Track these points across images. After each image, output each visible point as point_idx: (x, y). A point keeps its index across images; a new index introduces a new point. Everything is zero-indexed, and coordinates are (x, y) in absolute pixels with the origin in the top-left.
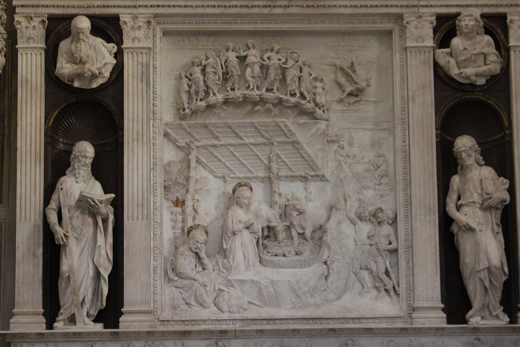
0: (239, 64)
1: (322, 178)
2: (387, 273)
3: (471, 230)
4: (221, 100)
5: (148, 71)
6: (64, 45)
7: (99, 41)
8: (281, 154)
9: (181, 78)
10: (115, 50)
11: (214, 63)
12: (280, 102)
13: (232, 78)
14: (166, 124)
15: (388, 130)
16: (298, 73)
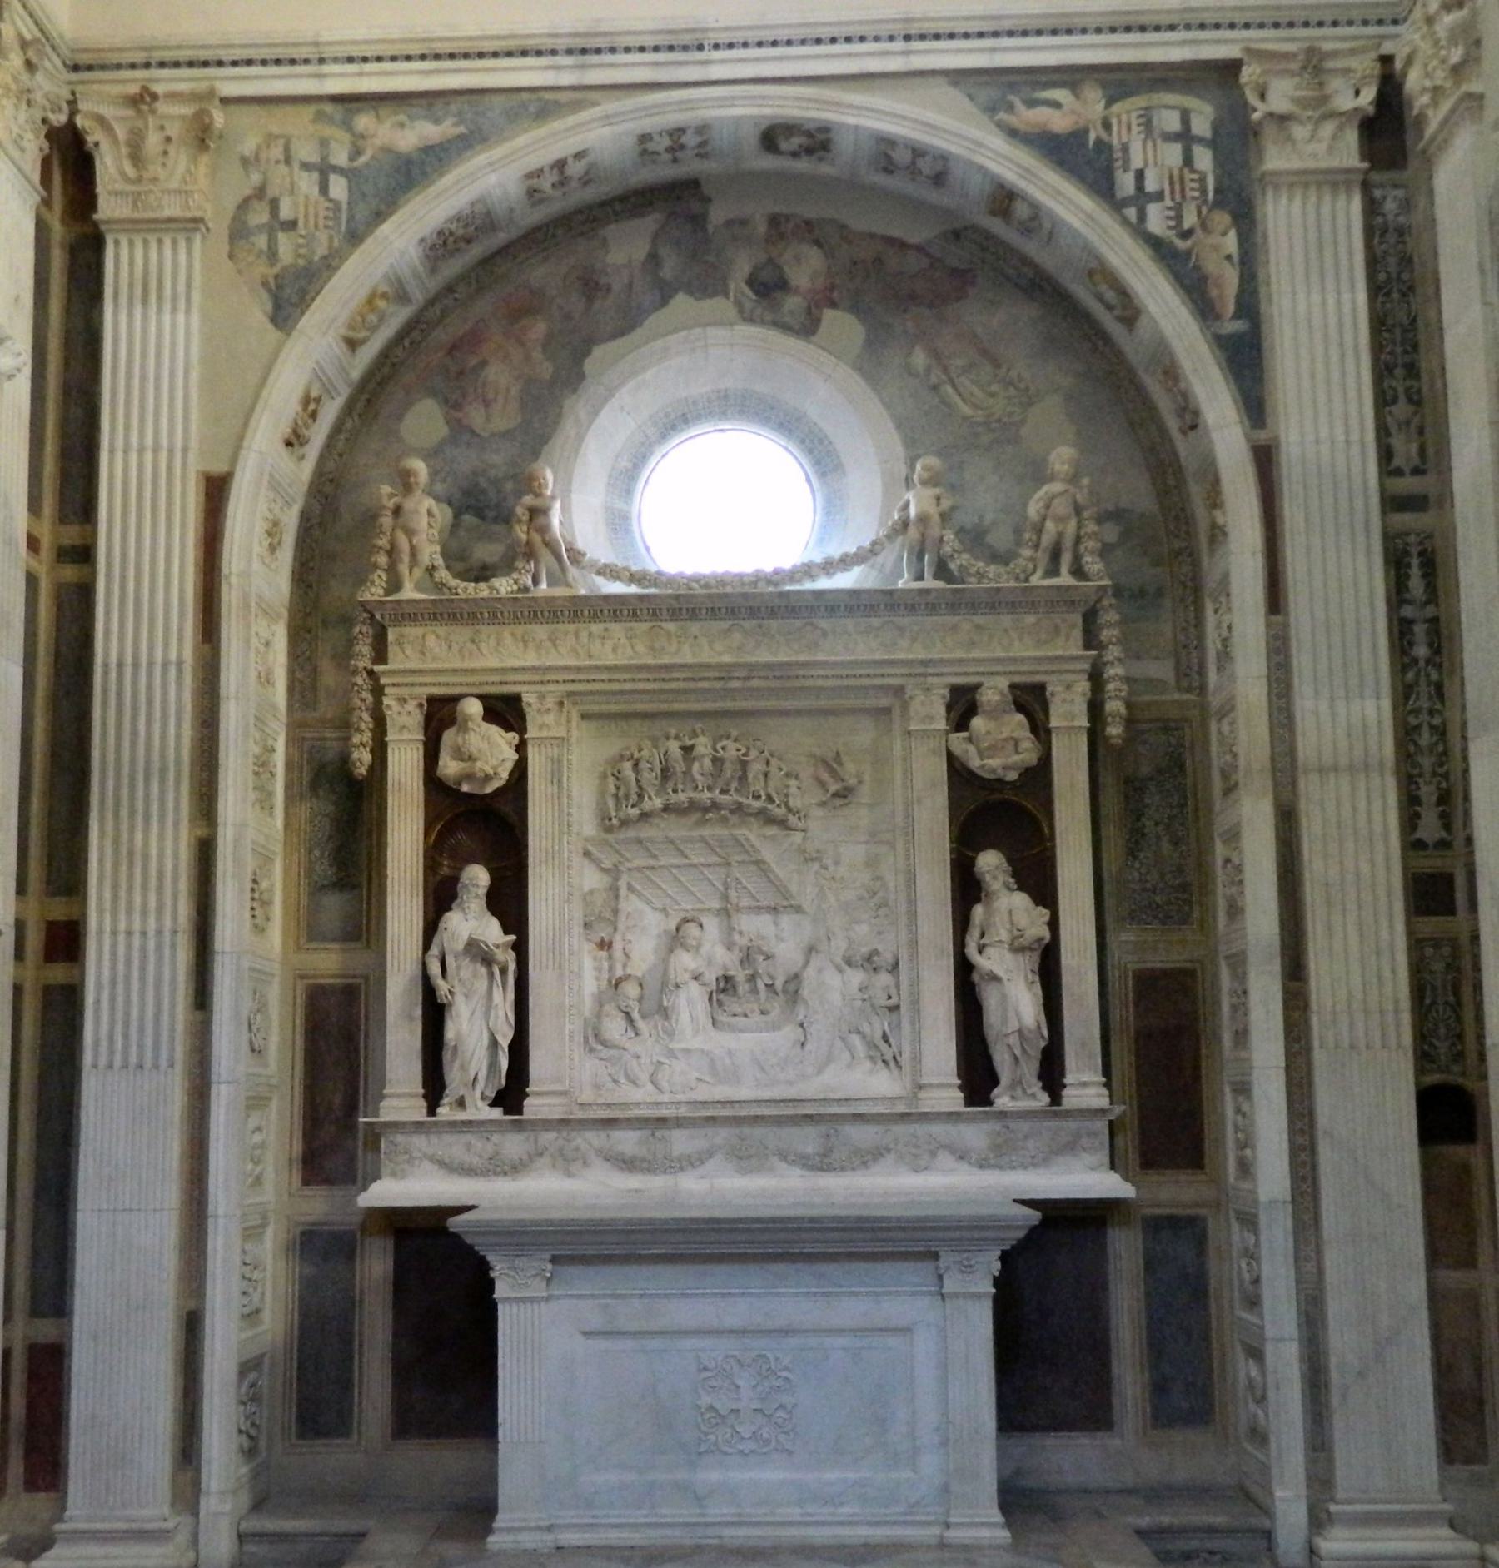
0: (685, 759)
1: (798, 909)
2: (885, 1038)
3: (995, 978)
5: (560, 771)
6: (449, 737)
7: (495, 731)
9: (604, 776)
10: (516, 741)
12: (738, 809)
14: (586, 840)
15: (888, 843)
16: (763, 767)
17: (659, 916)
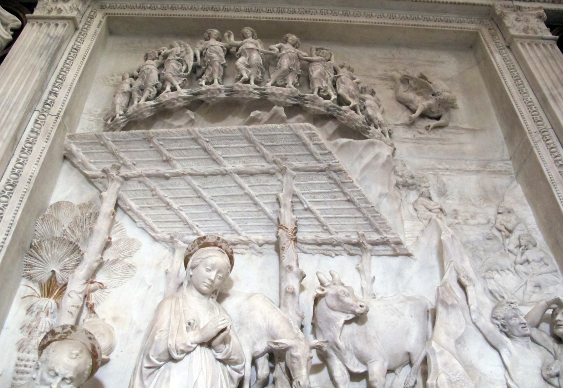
4: (185, 95)
8: (303, 194)
11: (182, 52)
13: (210, 67)
17: (161, 250)
